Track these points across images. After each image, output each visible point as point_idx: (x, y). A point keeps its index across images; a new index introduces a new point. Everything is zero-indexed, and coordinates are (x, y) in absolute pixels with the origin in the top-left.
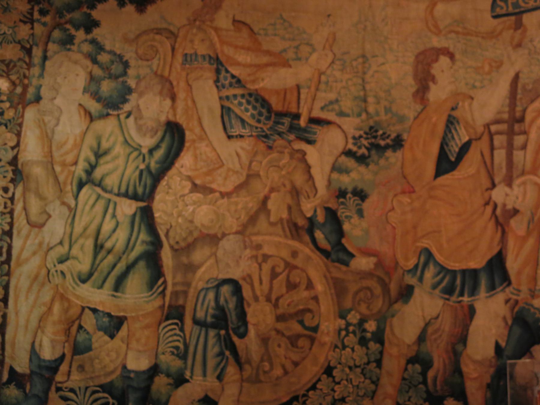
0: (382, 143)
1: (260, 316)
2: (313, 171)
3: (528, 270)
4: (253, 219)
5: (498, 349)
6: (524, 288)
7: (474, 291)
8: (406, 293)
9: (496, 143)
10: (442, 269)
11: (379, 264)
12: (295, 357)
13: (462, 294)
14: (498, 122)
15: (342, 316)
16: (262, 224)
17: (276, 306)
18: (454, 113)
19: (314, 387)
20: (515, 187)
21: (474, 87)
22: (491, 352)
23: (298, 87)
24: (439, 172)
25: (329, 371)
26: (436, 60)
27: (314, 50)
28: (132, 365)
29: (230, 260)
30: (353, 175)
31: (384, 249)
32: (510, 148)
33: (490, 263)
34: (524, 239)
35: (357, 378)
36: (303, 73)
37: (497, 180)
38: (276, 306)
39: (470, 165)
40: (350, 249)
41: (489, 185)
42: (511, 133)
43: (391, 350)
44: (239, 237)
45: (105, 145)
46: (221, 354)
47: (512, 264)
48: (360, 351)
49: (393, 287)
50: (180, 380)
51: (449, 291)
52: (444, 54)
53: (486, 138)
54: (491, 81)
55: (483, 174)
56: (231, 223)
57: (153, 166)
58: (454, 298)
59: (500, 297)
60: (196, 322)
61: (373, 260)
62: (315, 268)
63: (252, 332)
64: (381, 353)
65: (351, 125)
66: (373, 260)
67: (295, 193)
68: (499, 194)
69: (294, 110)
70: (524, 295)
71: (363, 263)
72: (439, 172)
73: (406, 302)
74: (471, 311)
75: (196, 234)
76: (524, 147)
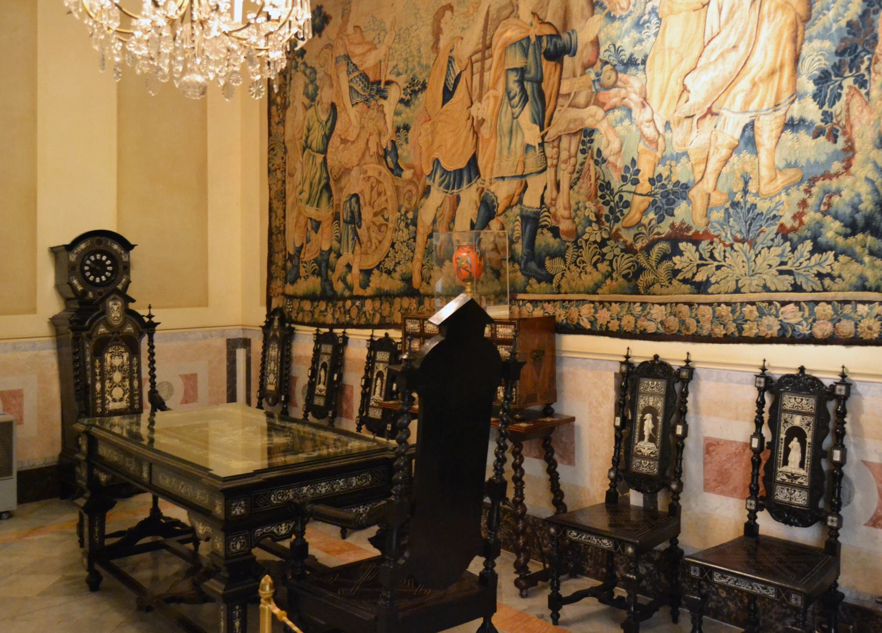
0: (417, 88)
1: (367, 214)
2: (387, 117)
3: (490, 166)
4: (363, 155)
5: (473, 226)
6: (487, 179)
7: (460, 186)
8: (427, 191)
9: (475, 70)
10: (445, 172)
11: (414, 174)
12: (380, 238)
13: (453, 188)
14: (476, 53)
15: (399, 211)
16: (367, 158)
17: (373, 207)
18: (451, 54)
19: (387, 256)
20: (483, 102)
21: (463, 29)
22: (468, 227)
23: (380, 61)
24: (445, 101)
25: (393, 245)
26: (443, 16)
27: (386, 33)
28: (323, 249)
29: (354, 184)
30: (404, 115)
31: (416, 163)
32: (482, 71)
33: (469, 163)
34: (488, 140)
35: (405, 249)
36: (382, 50)
37: (474, 98)
38: (373, 207)
39: (461, 92)
40: (402, 166)
41: (469, 104)
42: (483, 59)
43: (421, 230)
44: (358, 168)
45: (311, 124)
46: (353, 239)
47: (481, 163)
48: (406, 231)
49: (421, 188)
50: (339, 255)
51: (447, 187)
52: (448, 9)
53: (469, 68)
54: (473, 20)
55: (467, 94)
56: (355, 160)
57: (327, 132)
58: (450, 192)
59: (474, 187)
60: (344, 221)
61: (412, 171)
62: (388, 182)
63: (364, 225)
64: (415, 232)
65: (403, 81)
66: (412, 171)
67: (380, 134)
68: (474, 111)
69: (378, 79)
70: (487, 183)
71: (407, 174)
72: (445, 101)
73: (427, 198)
74: (458, 199)
75: (342, 170)
76: (490, 69)
